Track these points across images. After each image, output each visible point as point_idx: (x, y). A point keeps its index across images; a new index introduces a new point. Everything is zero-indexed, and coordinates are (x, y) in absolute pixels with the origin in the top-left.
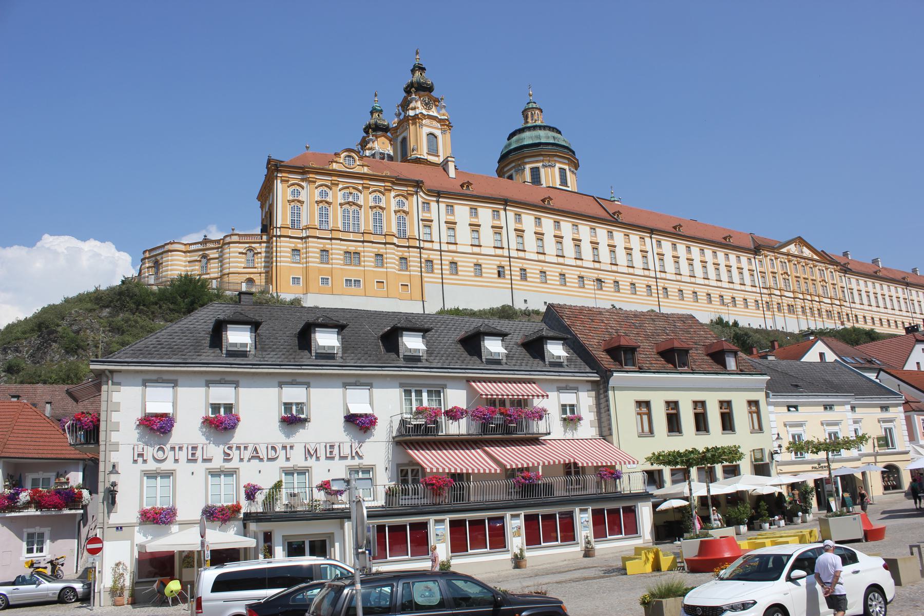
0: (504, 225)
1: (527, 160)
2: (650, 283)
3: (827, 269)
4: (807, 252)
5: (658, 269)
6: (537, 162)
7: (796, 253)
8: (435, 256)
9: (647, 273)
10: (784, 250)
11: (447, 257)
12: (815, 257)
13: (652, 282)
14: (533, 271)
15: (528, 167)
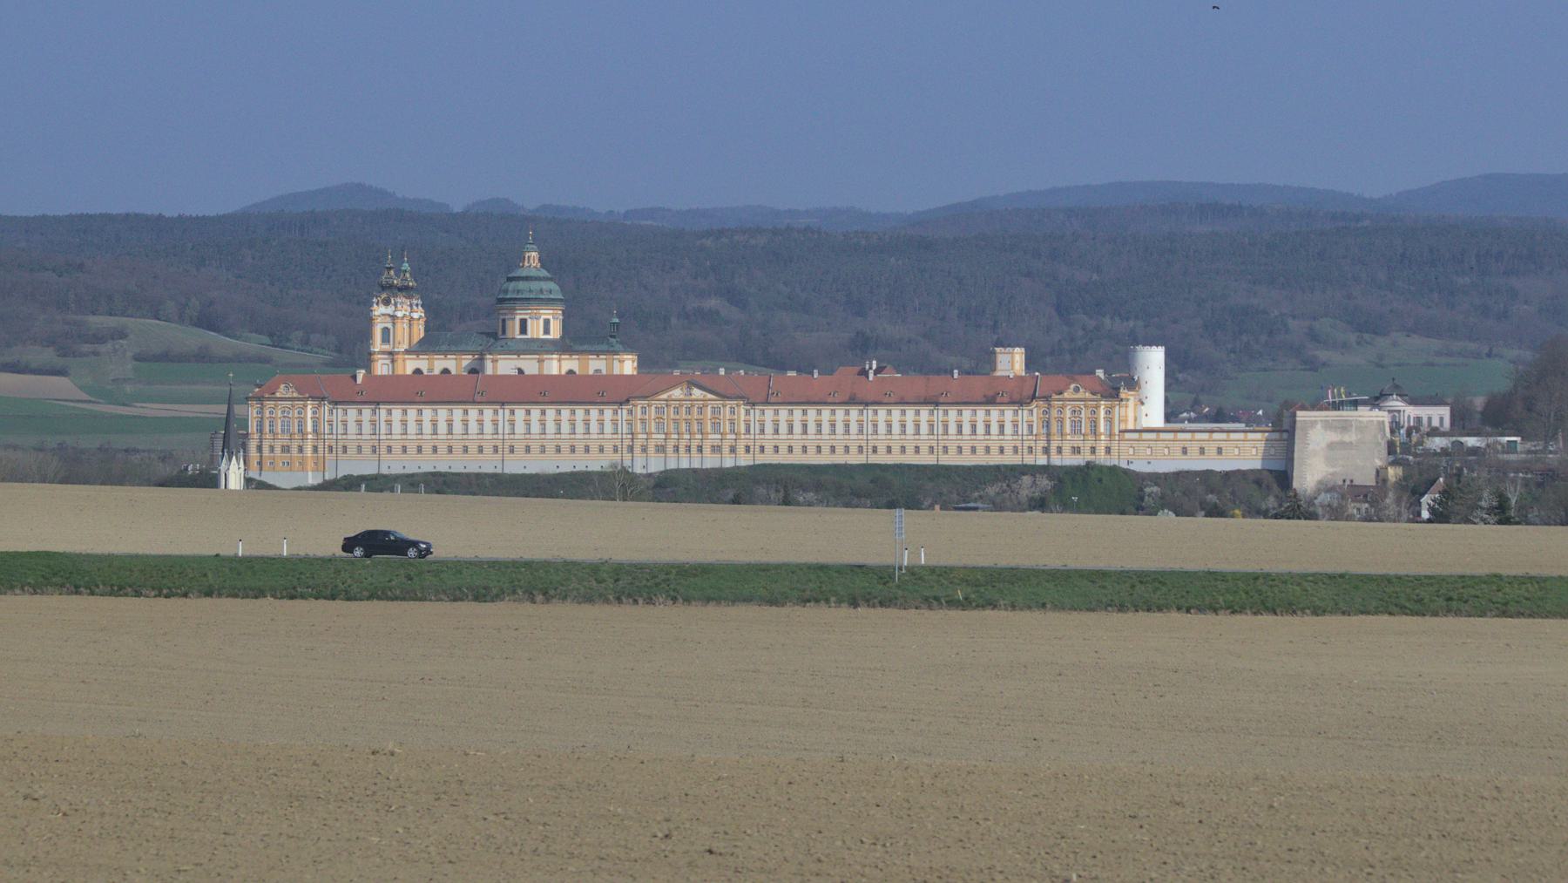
0: (377, 419)
1: (518, 312)
2: (498, 444)
3: (724, 406)
4: (697, 393)
5: (507, 432)
6: (524, 314)
7: (682, 397)
8: (333, 444)
9: (495, 436)
10: (665, 396)
11: (341, 444)
12: (710, 396)
13: (499, 444)
14: (397, 448)
15: (518, 317)
